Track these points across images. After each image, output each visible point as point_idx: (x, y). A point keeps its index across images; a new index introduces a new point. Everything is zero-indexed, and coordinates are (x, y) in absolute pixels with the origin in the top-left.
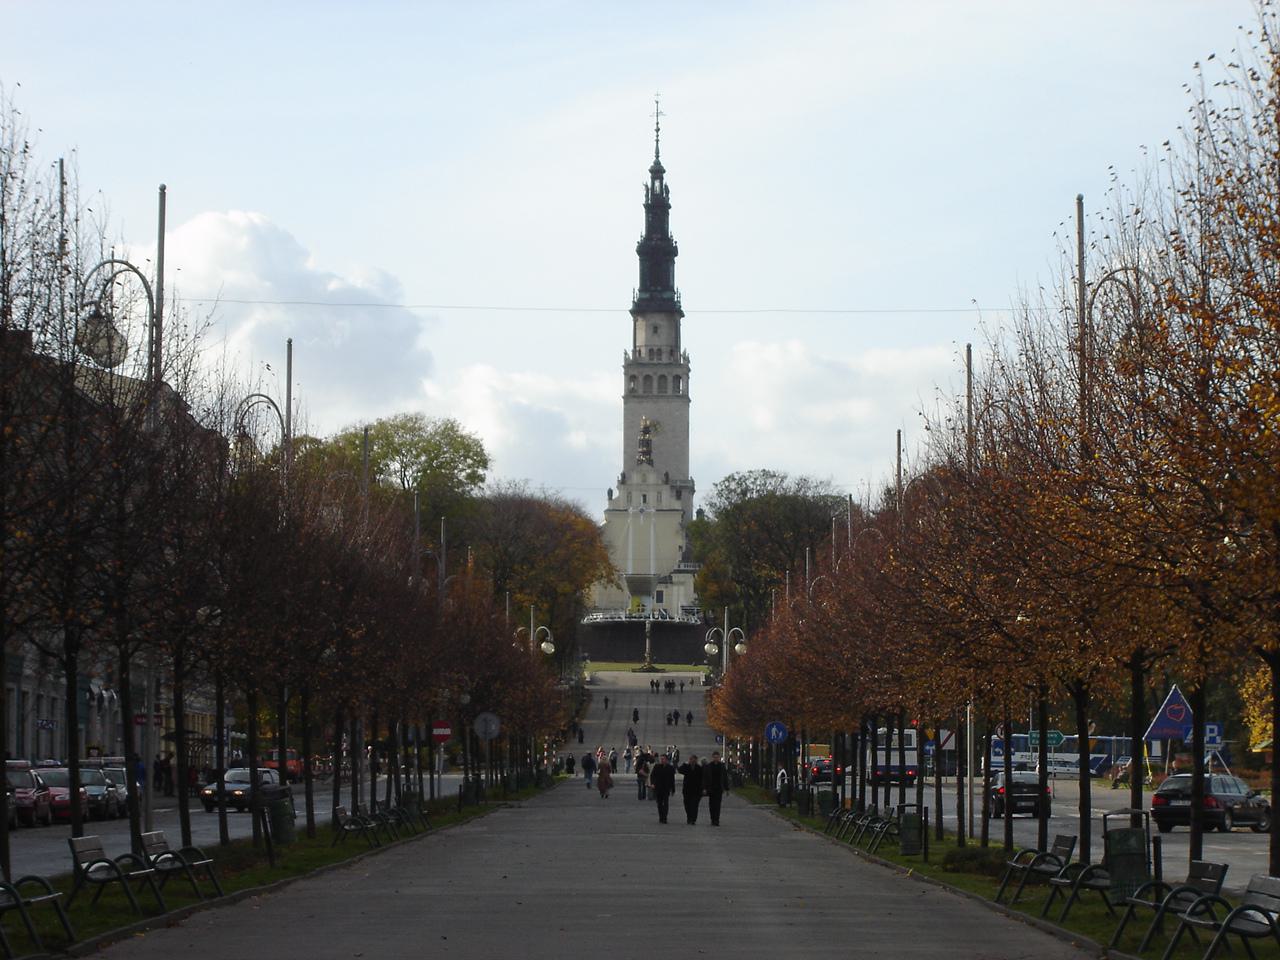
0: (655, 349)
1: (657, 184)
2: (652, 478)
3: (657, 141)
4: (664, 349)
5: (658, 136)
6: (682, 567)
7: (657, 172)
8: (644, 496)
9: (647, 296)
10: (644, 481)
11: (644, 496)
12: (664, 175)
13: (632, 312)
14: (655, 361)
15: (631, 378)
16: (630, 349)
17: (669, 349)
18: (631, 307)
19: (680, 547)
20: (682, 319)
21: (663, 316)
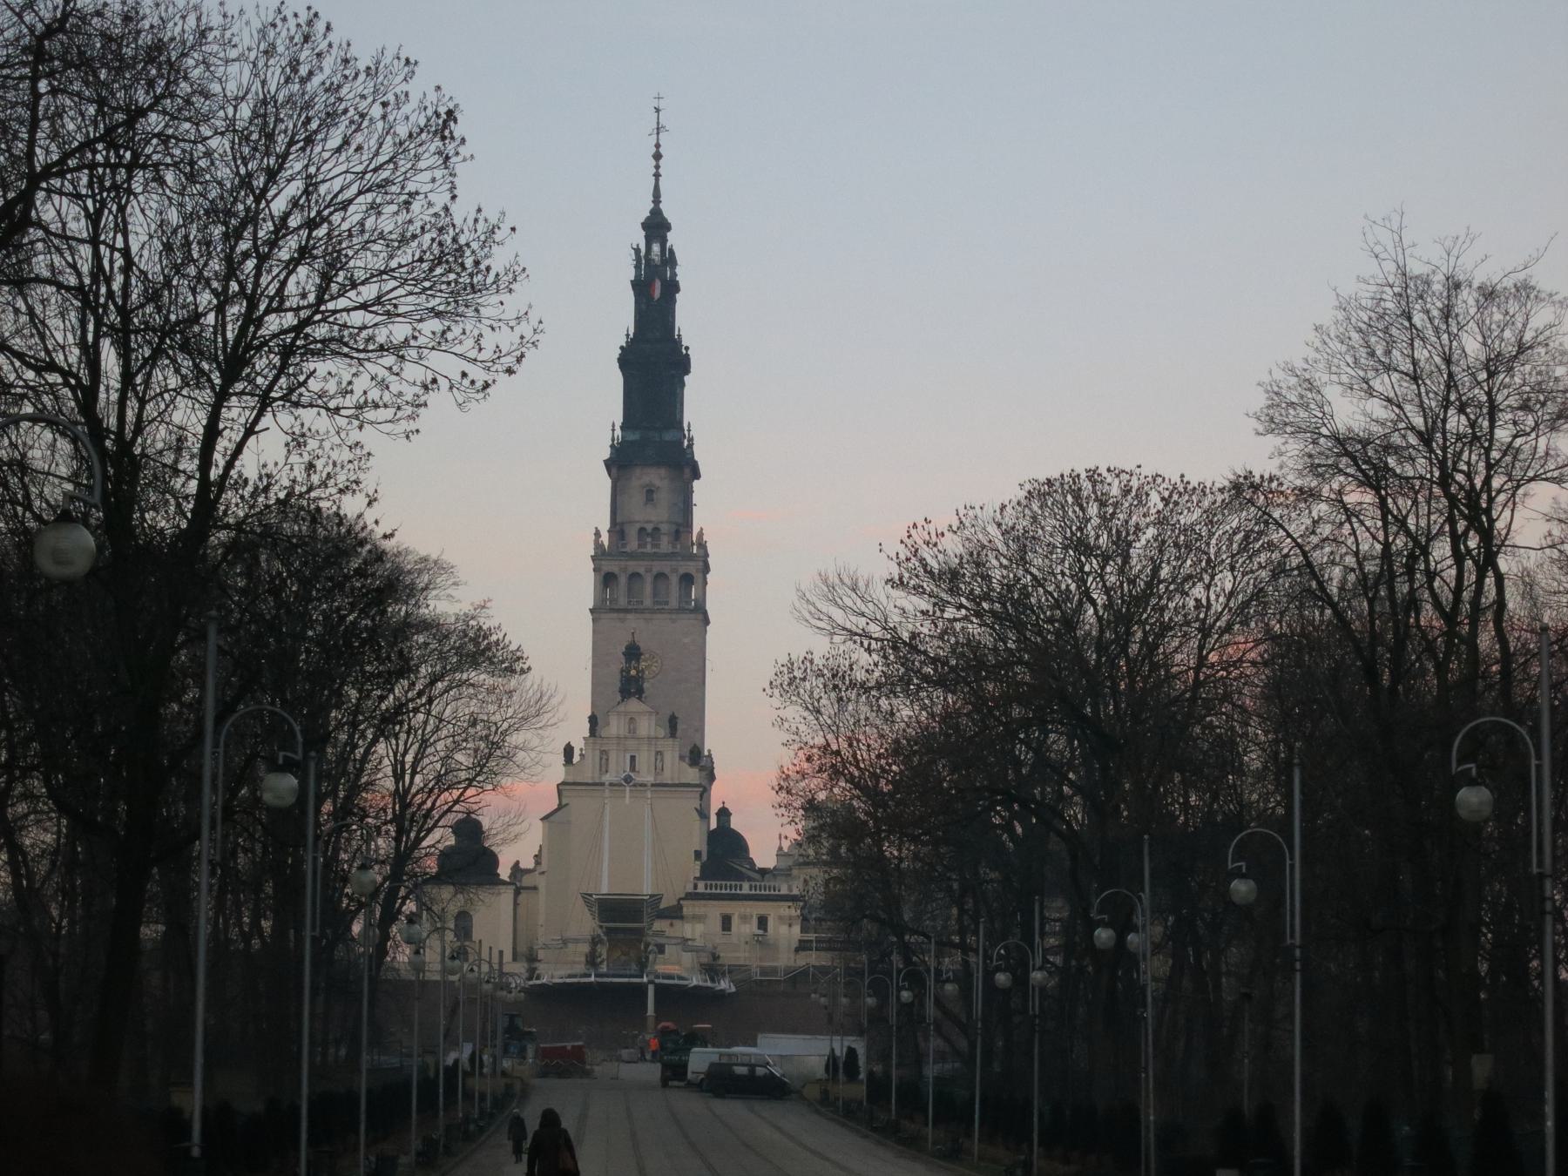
0: (649, 528)
1: (656, 248)
2: (646, 726)
3: (657, 176)
4: (664, 528)
5: (657, 167)
6: (701, 889)
7: (656, 226)
8: (633, 758)
9: (634, 436)
10: (632, 731)
11: (633, 758)
12: (669, 235)
13: (609, 464)
14: (649, 549)
15: (606, 580)
16: (605, 526)
17: (674, 527)
18: (607, 454)
19: (698, 854)
20: (696, 483)
21: (663, 471)
